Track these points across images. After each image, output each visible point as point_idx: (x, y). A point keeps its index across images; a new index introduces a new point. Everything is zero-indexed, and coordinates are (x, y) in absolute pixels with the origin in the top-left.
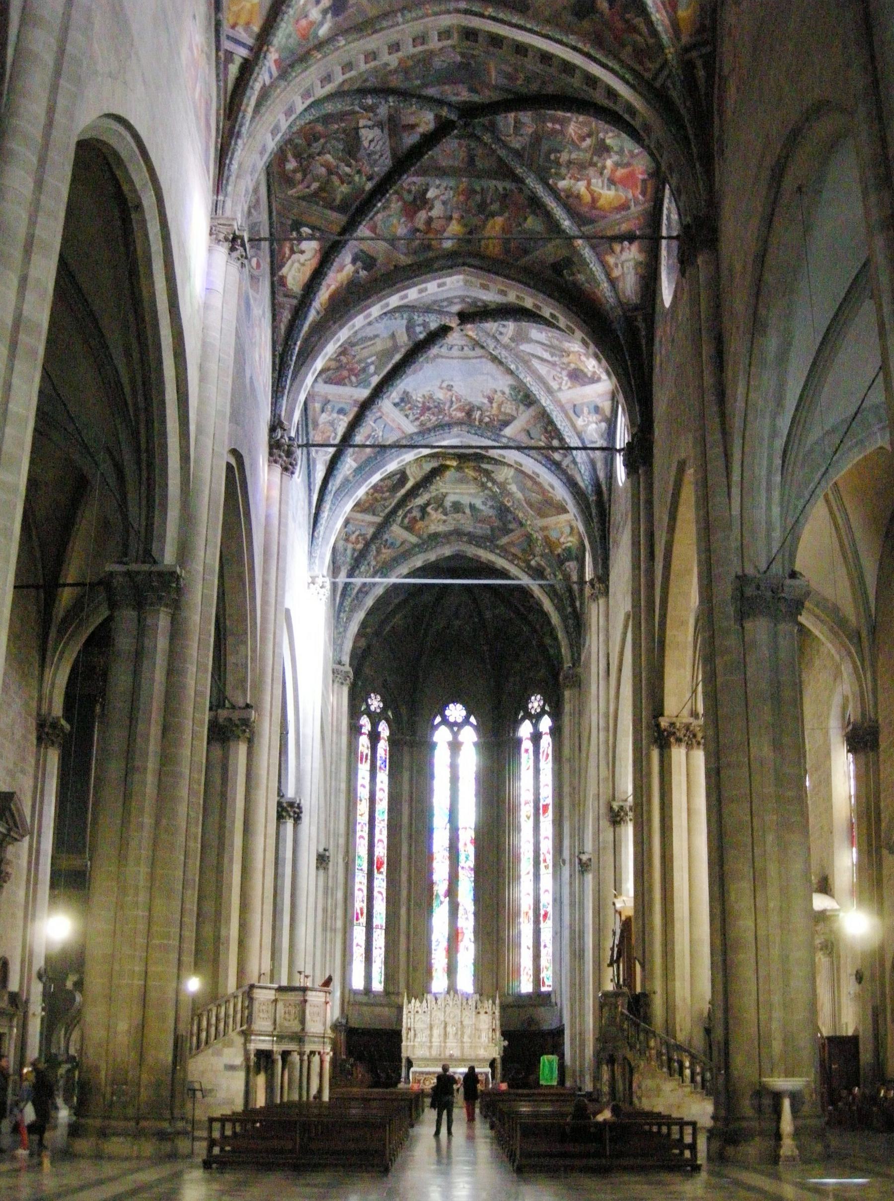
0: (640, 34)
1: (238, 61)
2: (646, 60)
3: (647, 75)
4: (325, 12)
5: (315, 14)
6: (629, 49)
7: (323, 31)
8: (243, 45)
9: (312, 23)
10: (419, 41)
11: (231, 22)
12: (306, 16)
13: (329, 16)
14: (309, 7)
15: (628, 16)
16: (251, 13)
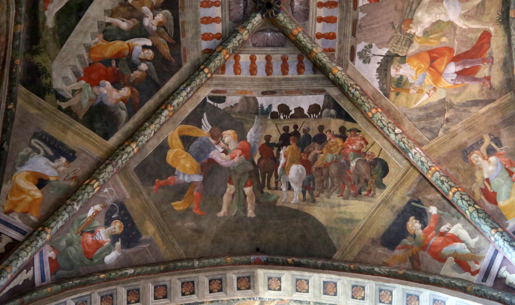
0: (461, 241)
1: (6, 241)
2: (472, 264)
3: (475, 279)
4: (114, 238)
5: (103, 235)
6: (451, 259)
7: (110, 258)
8: (16, 229)
9: (99, 244)
10: (215, 286)
11: (6, 208)
12: (93, 232)
13: (118, 244)
14: (97, 223)
15: (443, 229)
16: (31, 204)
